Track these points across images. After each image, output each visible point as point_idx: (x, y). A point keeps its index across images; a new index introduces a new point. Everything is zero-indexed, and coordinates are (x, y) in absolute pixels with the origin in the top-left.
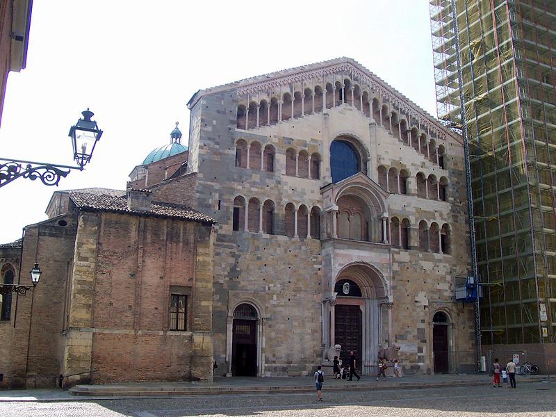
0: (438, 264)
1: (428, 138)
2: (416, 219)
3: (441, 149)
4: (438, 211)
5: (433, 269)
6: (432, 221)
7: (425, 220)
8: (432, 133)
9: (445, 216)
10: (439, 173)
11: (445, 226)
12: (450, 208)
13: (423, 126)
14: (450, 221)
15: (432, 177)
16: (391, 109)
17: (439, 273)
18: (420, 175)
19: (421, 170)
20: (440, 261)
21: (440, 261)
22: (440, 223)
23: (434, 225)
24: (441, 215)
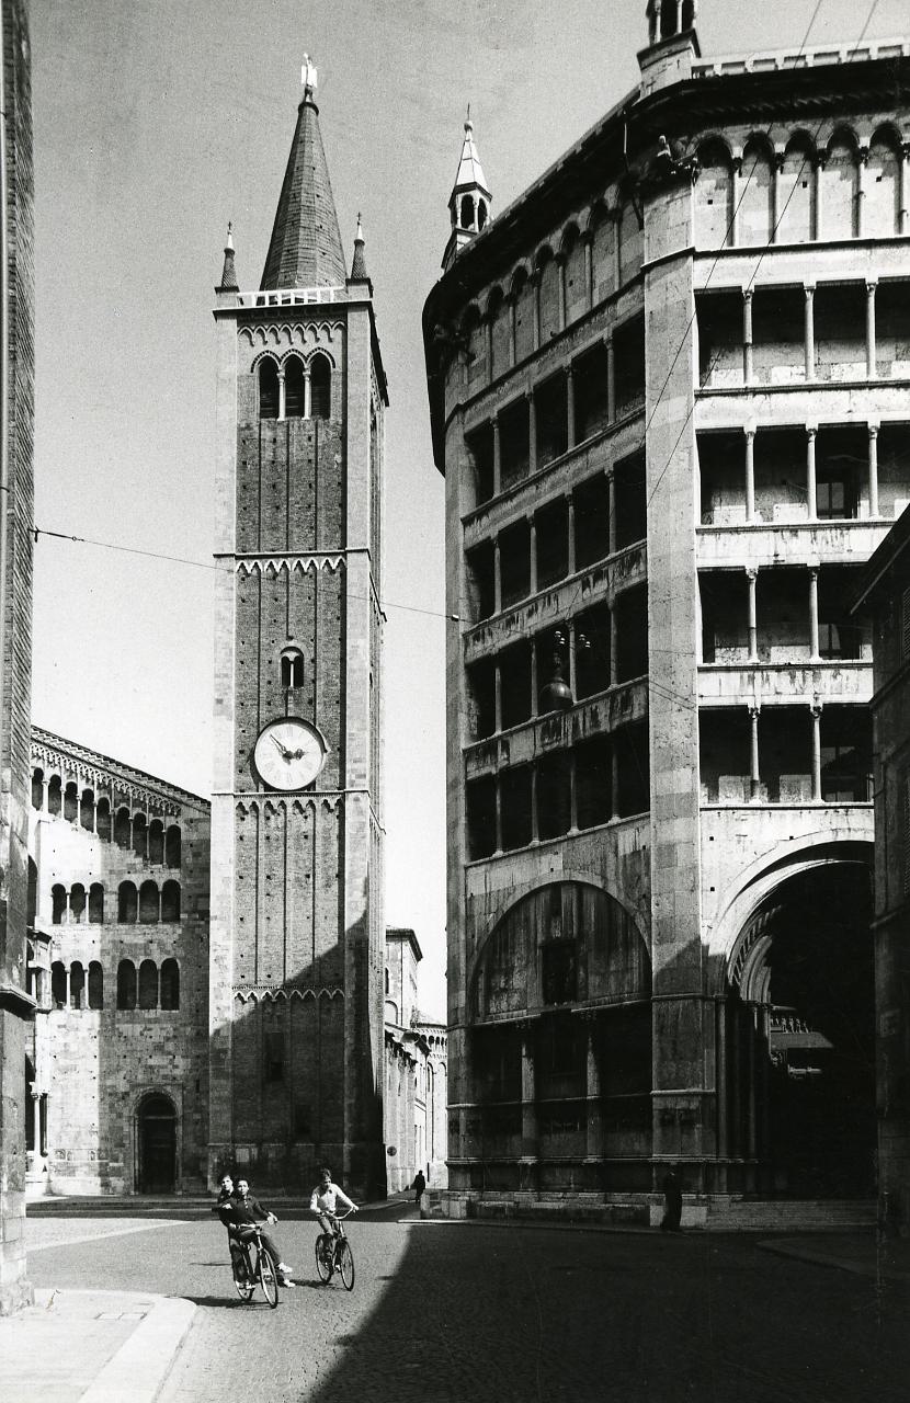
0: (149, 1026)
1: (150, 817)
2: (113, 958)
3: (175, 830)
4: (156, 940)
5: (142, 1034)
6: (142, 959)
7: (129, 958)
8: (154, 810)
9: (169, 948)
10: (161, 875)
11: (170, 965)
12: (180, 931)
13: (137, 803)
14: (181, 952)
15: (149, 886)
16: (82, 786)
17: (156, 1039)
18: (126, 889)
19: (127, 877)
20: (156, 1021)
21: (156, 1021)
22: (159, 959)
23: (148, 964)
24: (161, 945)
